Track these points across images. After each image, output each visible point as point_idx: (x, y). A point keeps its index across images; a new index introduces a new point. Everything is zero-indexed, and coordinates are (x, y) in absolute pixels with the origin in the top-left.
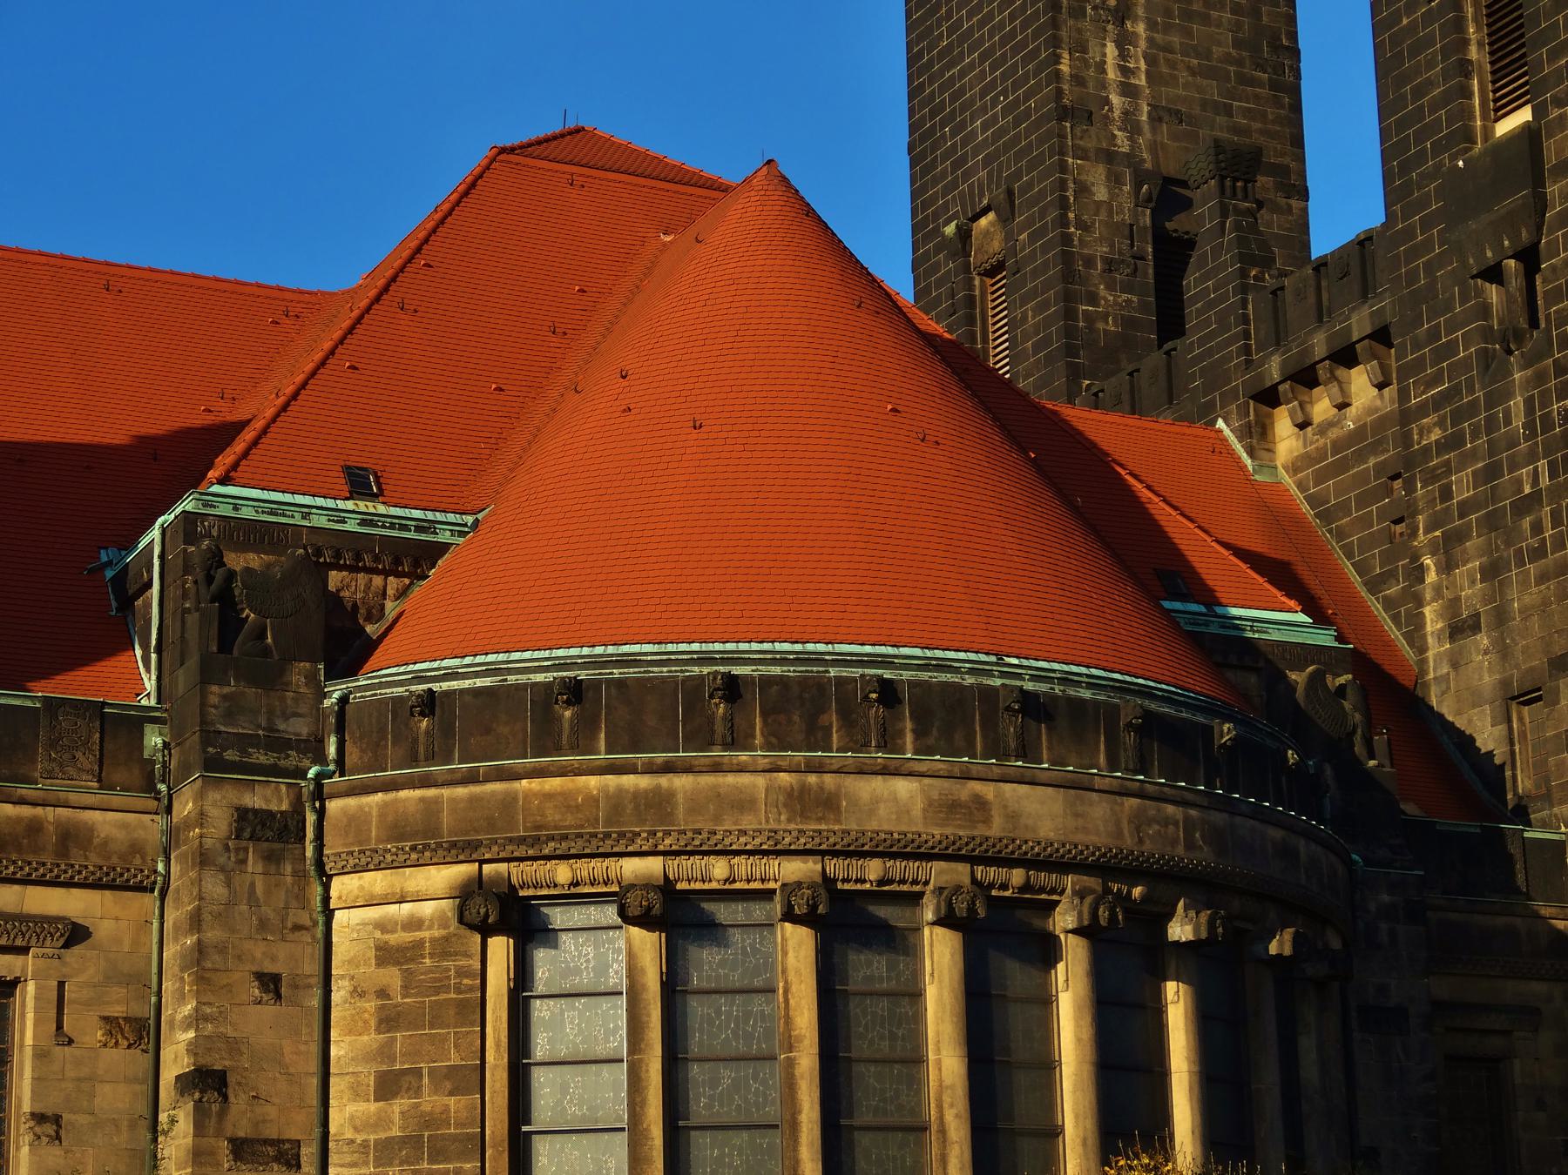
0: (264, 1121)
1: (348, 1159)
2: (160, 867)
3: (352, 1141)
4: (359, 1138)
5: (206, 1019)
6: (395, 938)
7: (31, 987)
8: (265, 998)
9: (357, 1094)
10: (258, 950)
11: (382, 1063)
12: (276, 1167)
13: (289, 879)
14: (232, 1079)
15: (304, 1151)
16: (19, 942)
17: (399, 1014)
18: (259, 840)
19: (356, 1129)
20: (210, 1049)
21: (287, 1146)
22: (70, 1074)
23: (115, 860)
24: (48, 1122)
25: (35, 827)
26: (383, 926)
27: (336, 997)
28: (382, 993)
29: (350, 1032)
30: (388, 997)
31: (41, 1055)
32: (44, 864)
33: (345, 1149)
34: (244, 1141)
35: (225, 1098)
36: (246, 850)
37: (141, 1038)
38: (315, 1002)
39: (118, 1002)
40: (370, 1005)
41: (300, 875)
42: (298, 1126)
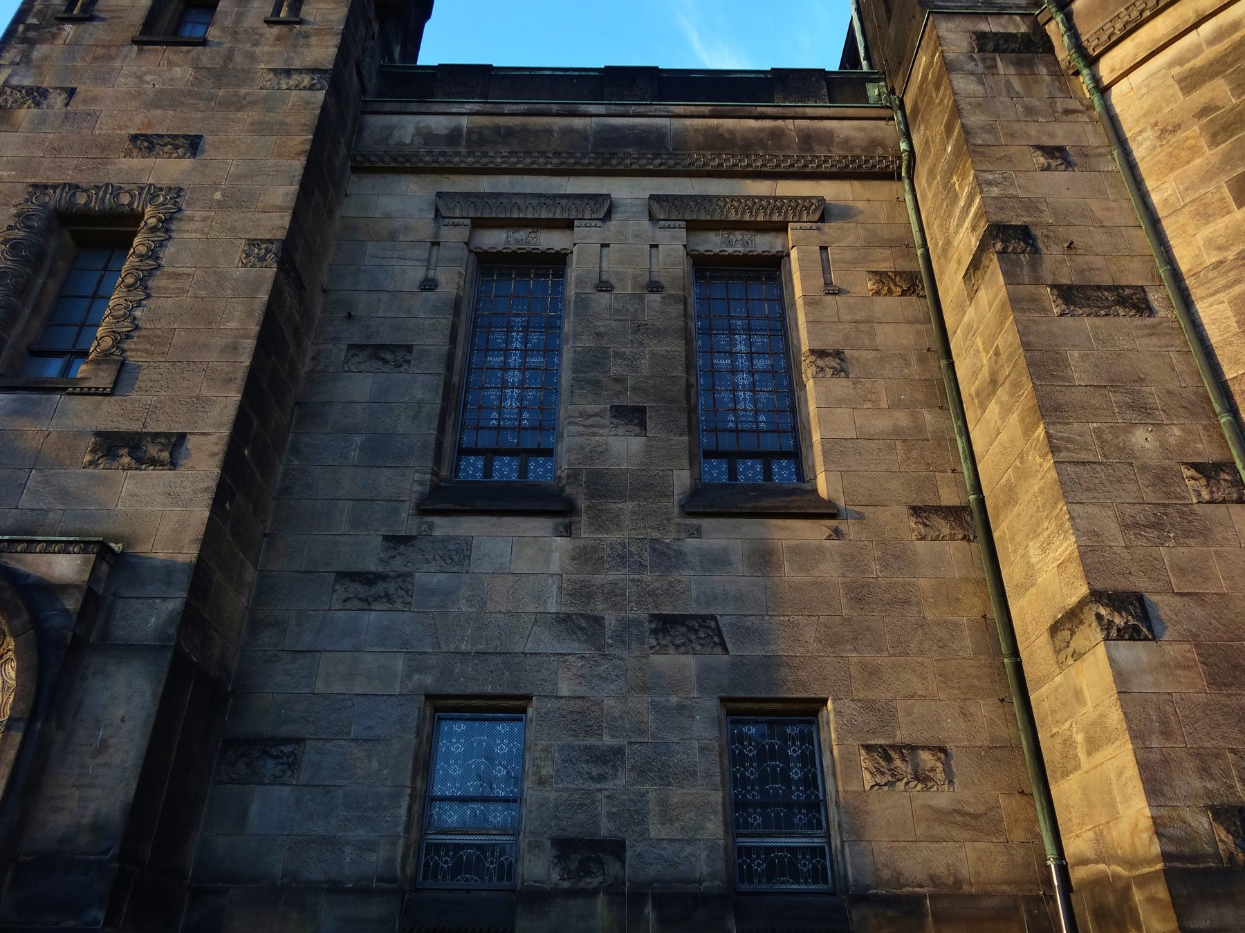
0: (1090, 269)
1: (1221, 282)
2: (903, 146)
3: (1221, 262)
4: (1231, 255)
5: (989, 183)
6: (1198, 62)
7: (794, 254)
8: (1054, 163)
9: (1205, 215)
10: (1033, 130)
11: (1234, 168)
12: (1121, 312)
13: (1047, 78)
14: (1037, 232)
15: (1154, 297)
16: (776, 218)
17: (1240, 113)
18: (1004, 51)
19: (1220, 248)
20: (1002, 208)
21: (1127, 291)
22: (846, 317)
23: (858, 151)
24: (833, 359)
25: (776, 134)
26: (1180, 61)
27: (1138, 153)
28: (1205, 111)
29: (1172, 169)
30: (1217, 108)
31: (811, 303)
32: (790, 157)
33: (1211, 275)
34: (1070, 287)
35: (1036, 251)
36: (994, 60)
37: (914, 285)
38: (1115, 164)
39: (884, 260)
40: (1194, 132)
41: (1058, 73)
42: (1133, 274)
